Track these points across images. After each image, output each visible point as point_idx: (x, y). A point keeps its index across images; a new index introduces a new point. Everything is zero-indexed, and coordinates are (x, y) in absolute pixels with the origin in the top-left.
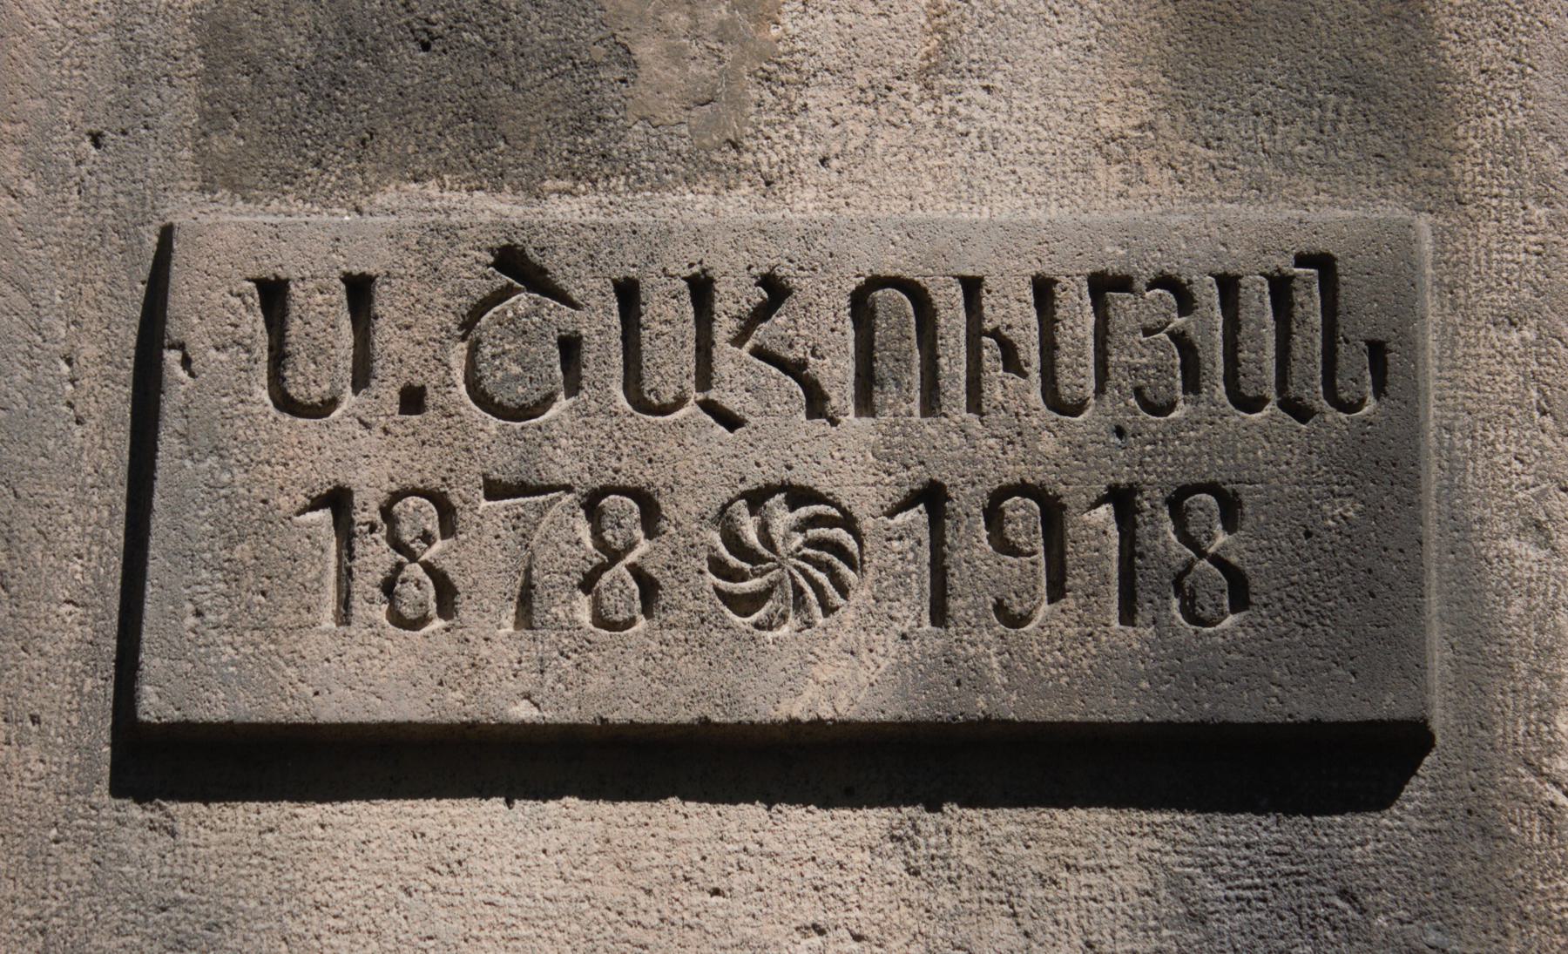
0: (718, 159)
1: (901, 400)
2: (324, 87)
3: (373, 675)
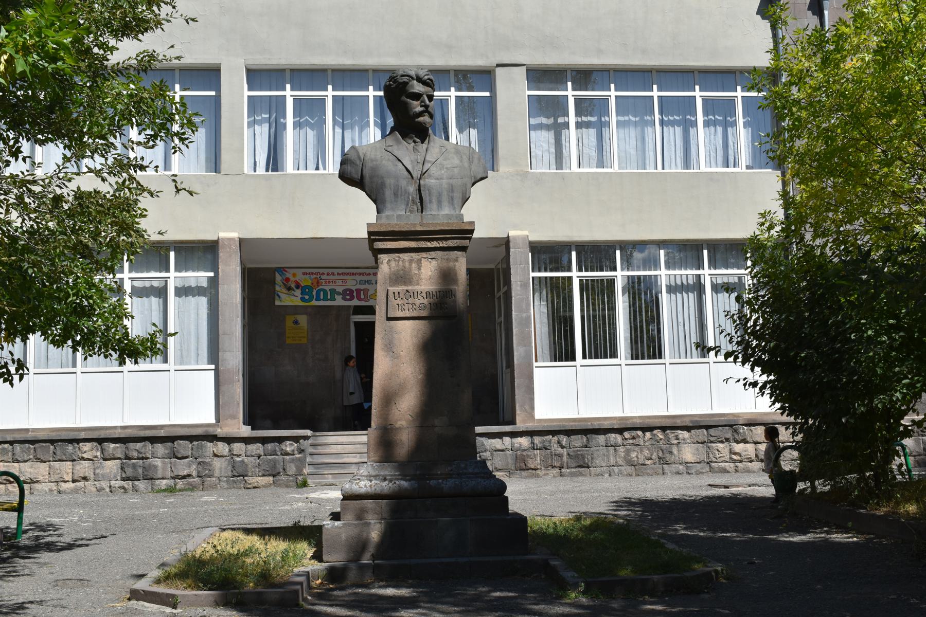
0: (418, 284)
2: (396, 281)
3: (400, 314)
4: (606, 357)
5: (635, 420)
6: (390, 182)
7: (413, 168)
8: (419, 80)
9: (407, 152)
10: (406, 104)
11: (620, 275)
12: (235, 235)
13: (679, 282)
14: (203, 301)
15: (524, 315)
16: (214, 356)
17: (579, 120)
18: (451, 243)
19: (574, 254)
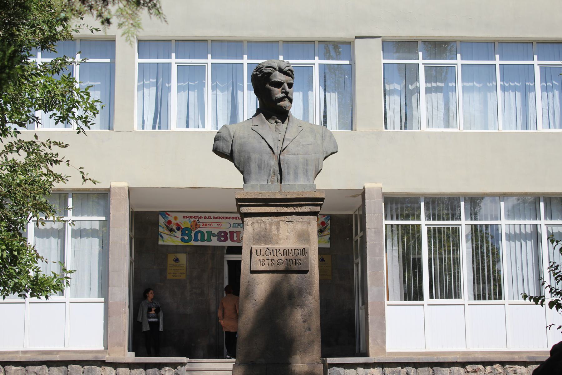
0: (277, 243)
1: (285, 255)
2: (258, 240)
4: (451, 297)
5: (476, 355)
6: (255, 157)
7: (275, 145)
8: (281, 70)
9: (270, 129)
10: (270, 91)
11: (464, 224)
12: (125, 184)
13: (518, 231)
14: (95, 243)
15: (378, 258)
16: (104, 289)
17: (429, 85)
18: (305, 209)
19: (422, 205)
